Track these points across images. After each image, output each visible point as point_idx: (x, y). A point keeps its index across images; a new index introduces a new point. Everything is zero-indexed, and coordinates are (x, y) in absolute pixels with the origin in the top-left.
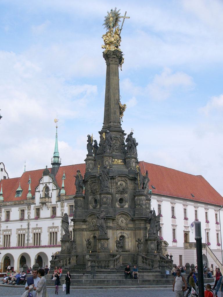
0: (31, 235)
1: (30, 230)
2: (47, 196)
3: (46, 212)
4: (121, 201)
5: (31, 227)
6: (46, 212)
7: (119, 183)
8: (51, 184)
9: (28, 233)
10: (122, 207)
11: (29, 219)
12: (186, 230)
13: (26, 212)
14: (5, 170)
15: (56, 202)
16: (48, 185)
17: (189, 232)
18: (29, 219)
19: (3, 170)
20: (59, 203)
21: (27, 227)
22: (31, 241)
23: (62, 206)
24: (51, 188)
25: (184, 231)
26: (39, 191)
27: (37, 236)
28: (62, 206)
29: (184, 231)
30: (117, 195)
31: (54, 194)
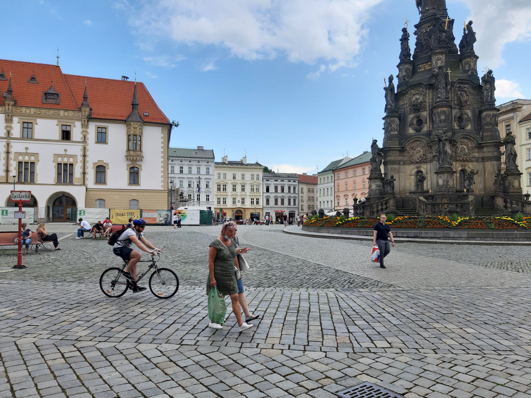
4: (460, 119)
10: (462, 128)
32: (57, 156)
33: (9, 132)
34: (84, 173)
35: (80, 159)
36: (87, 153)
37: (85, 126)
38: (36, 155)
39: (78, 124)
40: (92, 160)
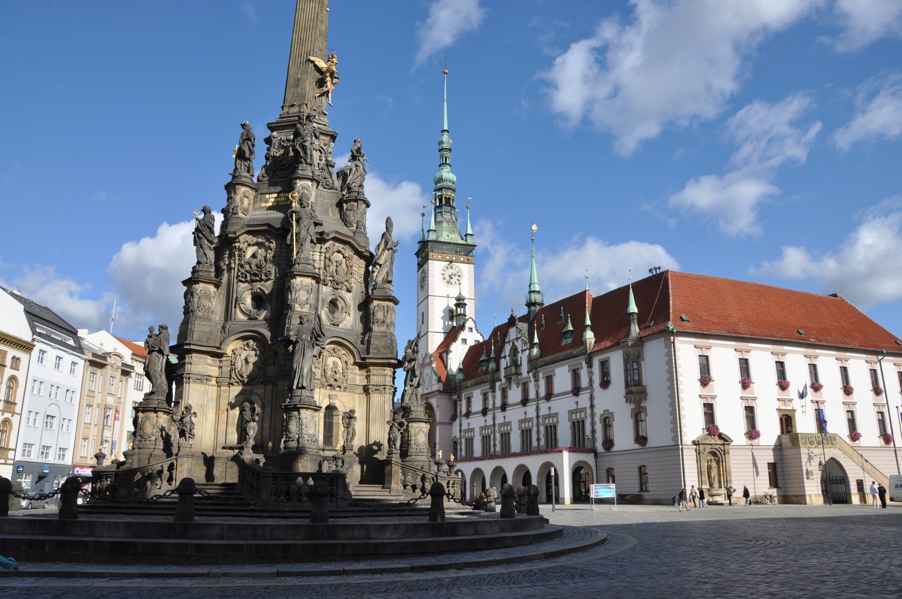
0: (498, 436)
1: (497, 428)
2: (516, 364)
3: (515, 394)
5: (497, 422)
6: (515, 394)
8: (520, 341)
11: (494, 408)
13: (490, 395)
14: (477, 330)
15: (528, 372)
17: (794, 411)
18: (494, 408)
19: (474, 330)
20: (531, 374)
21: (492, 423)
22: (498, 448)
23: (537, 380)
24: (519, 349)
25: (779, 410)
26: (505, 357)
27: (506, 437)
28: (537, 380)
29: (779, 410)
30: (243, 286)
31: (523, 358)
32: (571, 412)
33: (537, 392)
34: (593, 431)
35: (589, 411)
36: (595, 402)
38: (555, 415)
39: (584, 365)
40: (599, 411)
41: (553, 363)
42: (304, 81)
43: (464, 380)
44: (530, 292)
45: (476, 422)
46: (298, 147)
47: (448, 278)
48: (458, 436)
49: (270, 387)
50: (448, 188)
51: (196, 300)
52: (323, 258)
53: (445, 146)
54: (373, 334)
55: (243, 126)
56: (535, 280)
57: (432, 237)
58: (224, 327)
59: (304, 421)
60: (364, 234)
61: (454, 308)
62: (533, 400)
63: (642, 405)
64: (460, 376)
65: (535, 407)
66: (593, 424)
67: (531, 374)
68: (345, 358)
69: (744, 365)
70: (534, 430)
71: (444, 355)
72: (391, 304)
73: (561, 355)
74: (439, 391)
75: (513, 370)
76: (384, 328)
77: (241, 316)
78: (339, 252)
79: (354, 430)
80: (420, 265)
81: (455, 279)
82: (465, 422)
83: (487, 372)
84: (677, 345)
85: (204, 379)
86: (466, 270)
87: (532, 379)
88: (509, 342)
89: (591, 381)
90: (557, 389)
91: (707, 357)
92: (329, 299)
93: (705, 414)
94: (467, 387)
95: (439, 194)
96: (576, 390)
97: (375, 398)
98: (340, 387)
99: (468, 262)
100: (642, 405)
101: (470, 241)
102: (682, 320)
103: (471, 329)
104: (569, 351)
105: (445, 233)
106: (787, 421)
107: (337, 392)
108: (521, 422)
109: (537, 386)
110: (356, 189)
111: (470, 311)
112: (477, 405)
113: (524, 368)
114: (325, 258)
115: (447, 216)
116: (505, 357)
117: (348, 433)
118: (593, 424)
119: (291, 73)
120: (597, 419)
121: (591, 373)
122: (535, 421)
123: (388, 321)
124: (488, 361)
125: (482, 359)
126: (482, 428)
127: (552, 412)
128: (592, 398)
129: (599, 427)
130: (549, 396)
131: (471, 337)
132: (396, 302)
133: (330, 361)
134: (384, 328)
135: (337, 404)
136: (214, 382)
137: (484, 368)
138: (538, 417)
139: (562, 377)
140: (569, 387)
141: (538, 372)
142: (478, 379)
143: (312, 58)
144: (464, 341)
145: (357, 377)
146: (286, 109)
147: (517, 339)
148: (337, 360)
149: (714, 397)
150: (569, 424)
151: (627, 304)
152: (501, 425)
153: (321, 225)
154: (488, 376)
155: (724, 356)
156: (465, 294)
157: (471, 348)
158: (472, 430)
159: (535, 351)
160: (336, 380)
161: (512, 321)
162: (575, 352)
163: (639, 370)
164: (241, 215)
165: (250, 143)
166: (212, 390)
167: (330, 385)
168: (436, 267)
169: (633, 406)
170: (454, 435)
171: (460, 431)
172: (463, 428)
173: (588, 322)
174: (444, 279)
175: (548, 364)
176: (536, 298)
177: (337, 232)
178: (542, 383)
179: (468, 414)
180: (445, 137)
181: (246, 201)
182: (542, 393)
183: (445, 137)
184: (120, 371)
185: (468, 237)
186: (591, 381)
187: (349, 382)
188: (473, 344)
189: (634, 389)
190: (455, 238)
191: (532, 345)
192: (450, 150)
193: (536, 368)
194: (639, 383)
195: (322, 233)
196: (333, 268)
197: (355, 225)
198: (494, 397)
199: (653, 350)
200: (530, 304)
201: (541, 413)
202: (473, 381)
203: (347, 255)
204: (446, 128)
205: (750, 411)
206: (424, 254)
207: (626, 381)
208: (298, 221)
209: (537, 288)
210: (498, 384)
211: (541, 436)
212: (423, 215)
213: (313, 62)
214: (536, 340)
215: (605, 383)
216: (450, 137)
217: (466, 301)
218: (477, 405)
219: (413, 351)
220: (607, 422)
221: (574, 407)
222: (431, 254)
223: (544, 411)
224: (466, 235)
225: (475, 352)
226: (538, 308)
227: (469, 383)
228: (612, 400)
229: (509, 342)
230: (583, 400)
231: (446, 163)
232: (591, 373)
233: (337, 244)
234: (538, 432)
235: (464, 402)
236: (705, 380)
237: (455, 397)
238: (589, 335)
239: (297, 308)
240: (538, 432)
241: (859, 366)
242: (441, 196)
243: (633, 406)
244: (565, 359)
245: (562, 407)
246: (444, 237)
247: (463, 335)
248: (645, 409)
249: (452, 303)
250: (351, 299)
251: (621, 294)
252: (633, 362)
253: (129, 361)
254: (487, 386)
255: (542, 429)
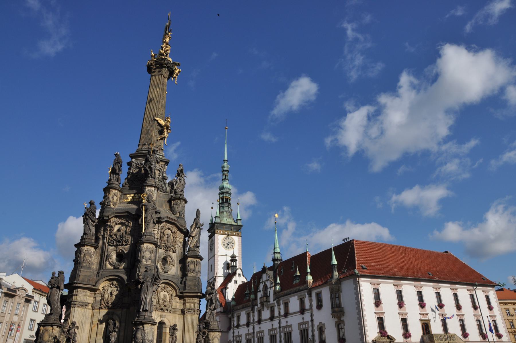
0: (256, 339)
1: (255, 334)
3: (266, 314)
5: (256, 331)
6: (266, 314)
7: (116, 229)
8: (269, 281)
9: (254, 337)
11: (254, 322)
12: (423, 319)
13: (251, 314)
14: (243, 275)
15: (274, 300)
16: (266, 283)
17: (429, 320)
18: (254, 322)
19: (241, 275)
20: (275, 302)
24: (269, 287)
25: (421, 320)
28: (279, 305)
29: (421, 320)
30: (111, 248)
31: (271, 292)
32: (300, 324)
33: (279, 312)
34: (313, 336)
35: (310, 323)
36: (314, 318)
37: (310, 296)
38: (291, 326)
40: (316, 323)
41: (288, 295)
42: (151, 131)
43: (235, 305)
44: (274, 253)
45: (243, 331)
46: (147, 168)
47: (226, 245)
48: (232, 340)
49: (125, 310)
50: (227, 193)
51: (82, 256)
52: (159, 232)
53: (225, 169)
54: (188, 278)
55: (116, 155)
56: (277, 245)
57: (218, 220)
58: (98, 273)
59: (146, 331)
60: (184, 219)
61: (230, 262)
62: (277, 317)
63: (342, 319)
64: (233, 303)
65: (278, 321)
66: (313, 331)
67: (275, 302)
68: (171, 293)
69: (399, 294)
70: (278, 335)
71: (224, 290)
72: (198, 260)
73: (293, 289)
74: (220, 312)
75: (265, 299)
76: (194, 275)
77: (109, 266)
78: (169, 229)
79: (176, 337)
80: (210, 237)
81: (230, 245)
82: (236, 331)
83: (249, 300)
84: (361, 283)
85: (84, 305)
86: (237, 240)
87: (276, 305)
88: (262, 282)
89: (311, 305)
90: (291, 310)
91: (378, 290)
92: (163, 257)
93: (379, 323)
94: (237, 310)
95: (221, 196)
96: (302, 311)
97: (188, 317)
98: (167, 310)
99: (238, 235)
100: (342, 319)
101: (239, 223)
102: (363, 268)
103: (239, 275)
104: (298, 288)
105: (225, 219)
106: (426, 327)
107: (165, 313)
108: (270, 330)
109: (279, 309)
110: (180, 193)
111: (239, 264)
112: (243, 320)
113: (272, 298)
114: (161, 232)
115: (226, 209)
116: (260, 291)
117: (172, 339)
118: (313, 331)
119: (144, 126)
120: (315, 328)
121: (311, 301)
122: (278, 330)
123: (197, 270)
124: (250, 294)
125: (246, 292)
126: (246, 335)
127: (288, 324)
128: (312, 315)
129: (316, 333)
130: (286, 314)
131: (240, 279)
132: (201, 259)
133: (162, 294)
134: (194, 275)
135: (166, 321)
136: (90, 307)
137: (248, 298)
138: (280, 327)
139: (294, 303)
140: (298, 308)
141: (280, 300)
142: (244, 305)
143: (157, 119)
144: (236, 282)
145: (178, 304)
146: (141, 146)
147: (267, 280)
148: (166, 293)
149: (383, 313)
150: (299, 331)
151: (331, 259)
152: (258, 333)
153: (159, 213)
154: (250, 303)
155: (388, 289)
156: (236, 254)
157: (240, 286)
158: (241, 336)
159: (278, 287)
160: (165, 306)
161: (264, 270)
162: (301, 288)
163: (339, 298)
164: (112, 206)
165: (119, 165)
166: (88, 312)
167: (162, 309)
168: (220, 238)
169: (337, 320)
170: (229, 339)
171: (233, 336)
172: (235, 335)
173: (309, 270)
174: (224, 245)
175: (285, 295)
176: (278, 256)
177: (168, 217)
178: (282, 307)
179: (238, 326)
180: (226, 164)
181: (115, 198)
182: (282, 313)
183: (226, 164)
184: (24, 299)
185: (238, 221)
186: (311, 305)
187: (173, 307)
188: (241, 283)
189: (336, 309)
190: (231, 221)
191: (276, 284)
192: (228, 171)
193: (278, 298)
194: (339, 306)
195: (159, 218)
196: (165, 238)
197: (178, 214)
198: (254, 315)
199: (347, 286)
200: (274, 260)
201: (282, 325)
202: (241, 306)
203: (173, 231)
204: (226, 159)
205: (404, 322)
206: (212, 231)
207: (332, 305)
208: (146, 211)
209: (278, 250)
210: (256, 307)
211: (282, 339)
212: (212, 208)
213: (157, 121)
214: (278, 281)
215: (320, 306)
216: (228, 164)
217: (237, 258)
218: (243, 320)
219: (212, 288)
220: (321, 329)
221: (301, 321)
222: (216, 230)
223: (283, 324)
224: (237, 220)
225: (242, 289)
226: (279, 262)
227: (238, 307)
228: (324, 316)
229: (262, 282)
230: (307, 317)
231: (226, 179)
232: (311, 301)
233: (168, 225)
234: (280, 337)
235: (235, 319)
236: (378, 303)
237: (230, 316)
238: (310, 278)
239: (144, 262)
240: (280, 337)
241: (463, 292)
242: (223, 197)
243: (337, 320)
244: (296, 292)
245: (294, 321)
246: (225, 221)
247: (235, 278)
248: (343, 321)
249: (229, 259)
250: (175, 257)
251: (327, 254)
252: (335, 294)
253: (30, 293)
254: (249, 309)
255: (282, 334)
